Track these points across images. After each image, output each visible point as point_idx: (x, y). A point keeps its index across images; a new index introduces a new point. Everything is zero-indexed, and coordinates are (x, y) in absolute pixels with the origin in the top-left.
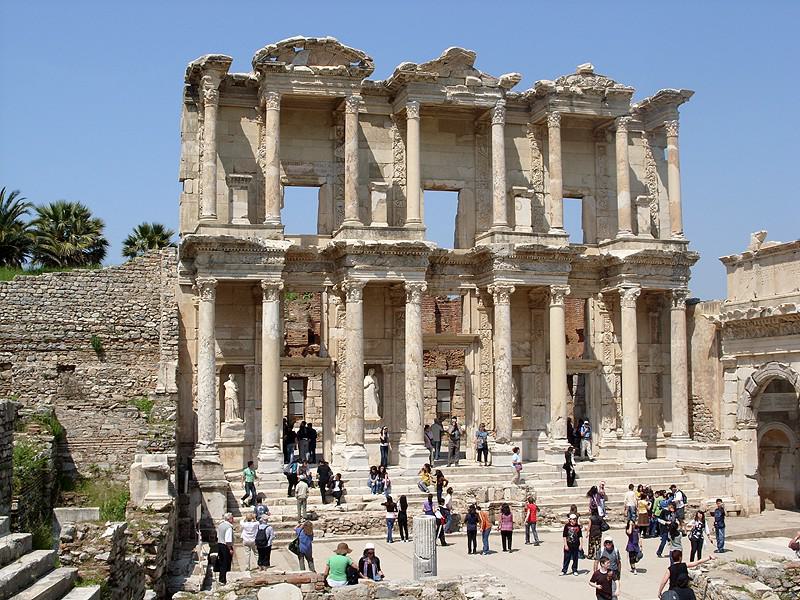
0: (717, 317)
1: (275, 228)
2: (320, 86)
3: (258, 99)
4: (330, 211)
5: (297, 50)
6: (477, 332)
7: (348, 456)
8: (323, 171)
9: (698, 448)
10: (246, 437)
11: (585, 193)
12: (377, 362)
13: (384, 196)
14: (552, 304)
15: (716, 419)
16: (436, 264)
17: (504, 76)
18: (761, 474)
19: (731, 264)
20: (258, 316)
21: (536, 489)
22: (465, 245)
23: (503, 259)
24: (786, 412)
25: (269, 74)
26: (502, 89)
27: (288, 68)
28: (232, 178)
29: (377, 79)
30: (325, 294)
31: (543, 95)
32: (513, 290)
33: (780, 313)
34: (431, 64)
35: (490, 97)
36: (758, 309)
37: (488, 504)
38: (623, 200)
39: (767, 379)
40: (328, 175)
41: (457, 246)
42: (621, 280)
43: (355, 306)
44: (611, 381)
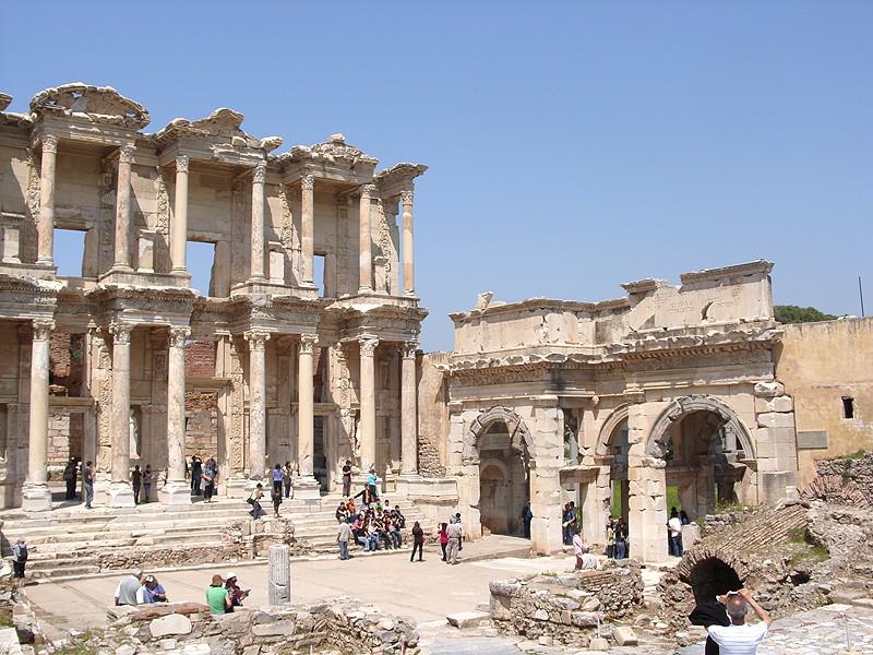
0: (447, 367)
1: (48, 268)
2: (96, 133)
3: (30, 141)
4: (96, 255)
5: (76, 96)
6: (229, 376)
7: (114, 494)
8: (89, 216)
9: (429, 483)
10: (8, 476)
11: (328, 251)
12: (137, 402)
13: (151, 244)
14: (302, 351)
15: (442, 457)
16: (198, 311)
17: (268, 139)
18: (481, 506)
19: (459, 320)
20: (27, 356)
21: (293, 522)
22: (220, 294)
23: (261, 309)
24: (502, 450)
25: (47, 116)
26: (264, 151)
27: (67, 113)
28: (5, 217)
29: (147, 133)
30: (88, 336)
31: (299, 159)
32: (268, 338)
33: (508, 364)
34: (203, 121)
35: (254, 158)
36: (488, 360)
37: (252, 537)
38: (365, 259)
39: (491, 421)
40: (95, 220)
41: (212, 294)
42: (361, 331)
43: (122, 348)
44: (347, 423)
